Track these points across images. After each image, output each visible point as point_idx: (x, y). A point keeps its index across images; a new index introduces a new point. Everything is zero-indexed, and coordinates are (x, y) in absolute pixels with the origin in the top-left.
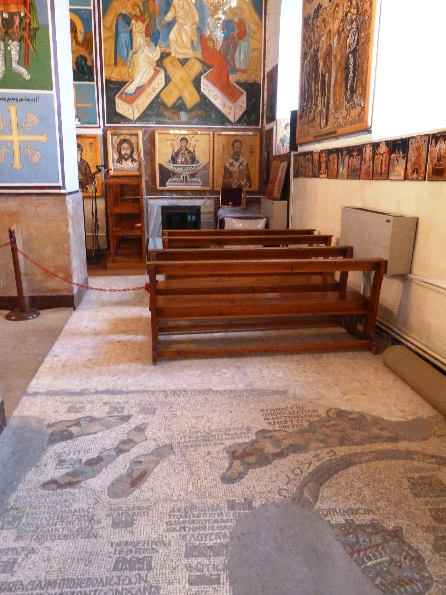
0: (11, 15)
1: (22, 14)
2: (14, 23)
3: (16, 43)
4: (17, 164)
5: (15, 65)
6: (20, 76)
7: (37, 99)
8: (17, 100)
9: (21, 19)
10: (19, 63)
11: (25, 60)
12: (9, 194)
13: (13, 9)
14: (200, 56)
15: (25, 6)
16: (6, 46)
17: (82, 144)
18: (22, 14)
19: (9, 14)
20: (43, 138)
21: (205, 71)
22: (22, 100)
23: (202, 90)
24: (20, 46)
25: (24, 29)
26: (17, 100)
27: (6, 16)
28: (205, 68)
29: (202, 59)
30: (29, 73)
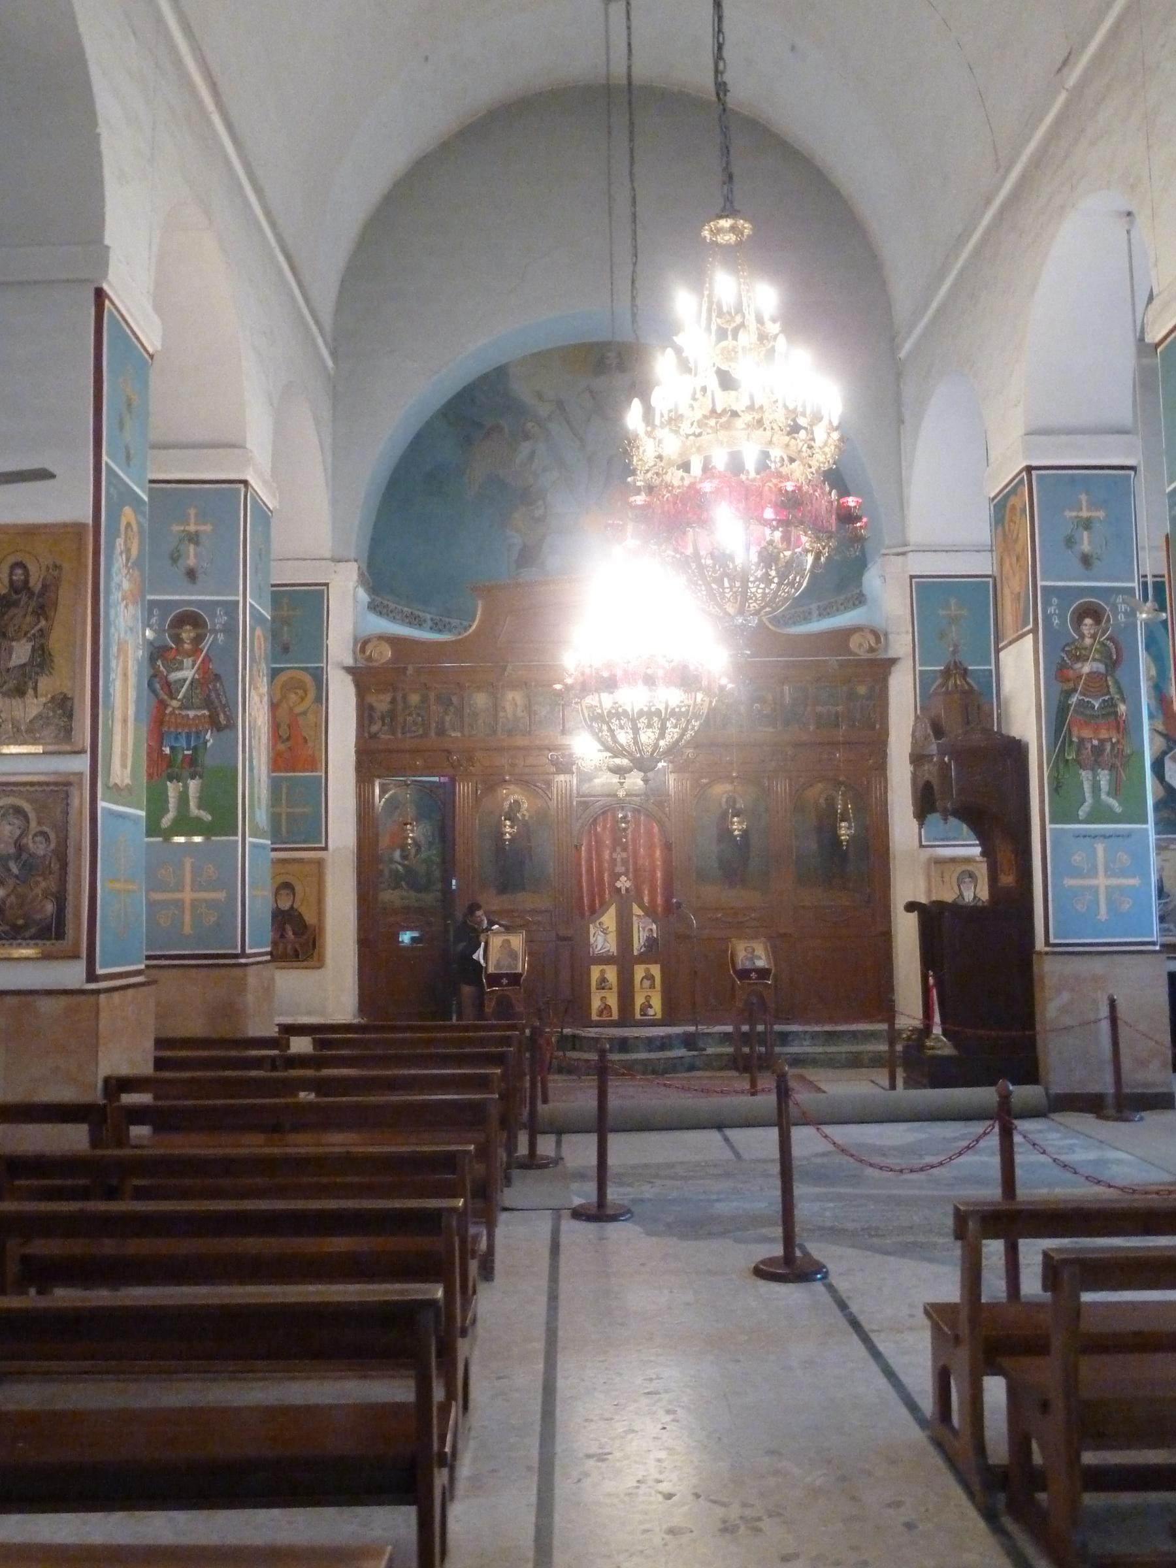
0: (1102, 742)
1: (1114, 740)
2: (1104, 750)
3: (1106, 772)
4: (1103, 914)
5: (1103, 796)
6: (1110, 808)
7: (1128, 835)
8: (1104, 837)
9: (1113, 745)
10: (1108, 794)
11: (1115, 791)
12: (1090, 953)
13: (1104, 734)
14: (1161, 728)
15: (1118, 732)
16: (1095, 776)
17: (977, 873)
18: (1114, 740)
19: (1099, 740)
20: (1134, 882)
21: (1171, 749)
22: (1111, 836)
23: (1167, 778)
24: (1111, 775)
25: (1116, 756)
26: (1104, 837)
27: (1095, 742)
28: (1171, 744)
29: (1165, 732)
30: (1120, 804)
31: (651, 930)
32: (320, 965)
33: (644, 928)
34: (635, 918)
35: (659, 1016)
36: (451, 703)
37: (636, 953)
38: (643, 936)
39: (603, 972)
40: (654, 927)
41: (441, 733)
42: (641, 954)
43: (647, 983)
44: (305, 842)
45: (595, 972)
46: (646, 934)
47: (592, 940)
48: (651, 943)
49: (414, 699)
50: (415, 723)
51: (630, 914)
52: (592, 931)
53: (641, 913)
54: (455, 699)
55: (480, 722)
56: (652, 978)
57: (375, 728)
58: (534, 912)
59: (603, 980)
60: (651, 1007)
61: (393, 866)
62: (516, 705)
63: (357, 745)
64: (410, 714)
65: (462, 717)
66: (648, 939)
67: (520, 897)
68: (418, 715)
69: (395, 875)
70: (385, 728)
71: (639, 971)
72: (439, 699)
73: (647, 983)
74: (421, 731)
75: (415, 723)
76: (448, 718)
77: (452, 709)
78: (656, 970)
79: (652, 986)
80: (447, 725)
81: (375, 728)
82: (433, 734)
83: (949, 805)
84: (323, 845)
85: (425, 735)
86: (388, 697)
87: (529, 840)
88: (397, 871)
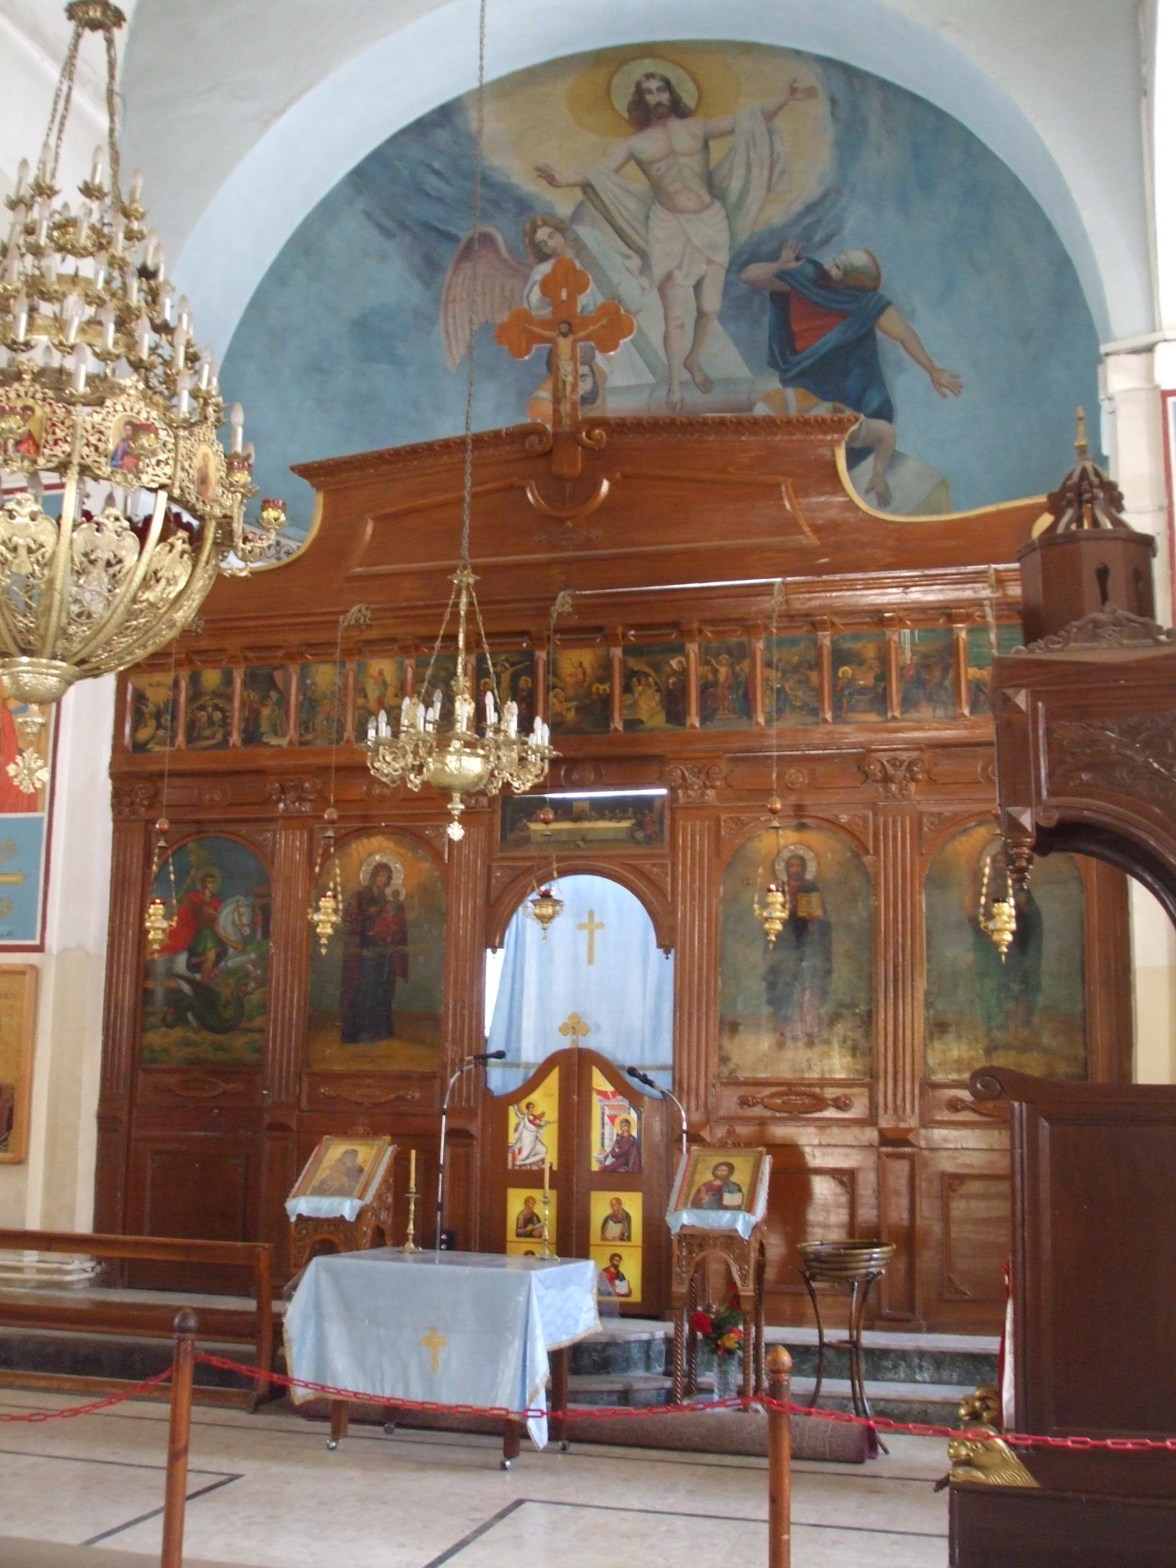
31: (627, 1122)
32: (20, 1161)
33: (612, 1119)
34: (596, 1099)
35: (636, 1297)
36: (272, 684)
37: (595, 1167)
38: (612, 1133)
39: (529, 1202)
40: (633, 1116)
41: (251, 737)
42: (605, 1170)
43: (614, 1229)
44: (10, 935)
45: (516, 1202)
46: (617, 1130)
47: (512, 1137)
48: (626, 1148)
49: (211, 678)
50: (211, 723)
51: (590, 1089)
52: (513, 1119)
53: (609, 1088)
54: (278, 676)
55: (320, 717)
56: (625, 1219)
57: (143, 734)
58: (405, 1077)
59: (530, 1219)
60: (622, 1278)
61: (173, 984)
62: (385, 684)
63: (113, 764)
64: (202, 708)
65: (287, 712)
66: (621, 1140)
67: (383, 1046)
68: (216, 707)
69: (175, 997)
70: (161, 732)
71: (600, 1205)
72: (251, 680)
73: (614, 1229)
74: (219, 737)
75: (211, 723)
76: (266, 712)
77: (274, 695)
78: (633, 1204)
79: (625, 1237)
80: (265, 727)
81: (143, 734)
82: (235, 738)
83: (1026, 820)
84: (37, 942)
85: (225, 742)
86: (168, 678)
87: (404, 941)
88: (179, 991)
